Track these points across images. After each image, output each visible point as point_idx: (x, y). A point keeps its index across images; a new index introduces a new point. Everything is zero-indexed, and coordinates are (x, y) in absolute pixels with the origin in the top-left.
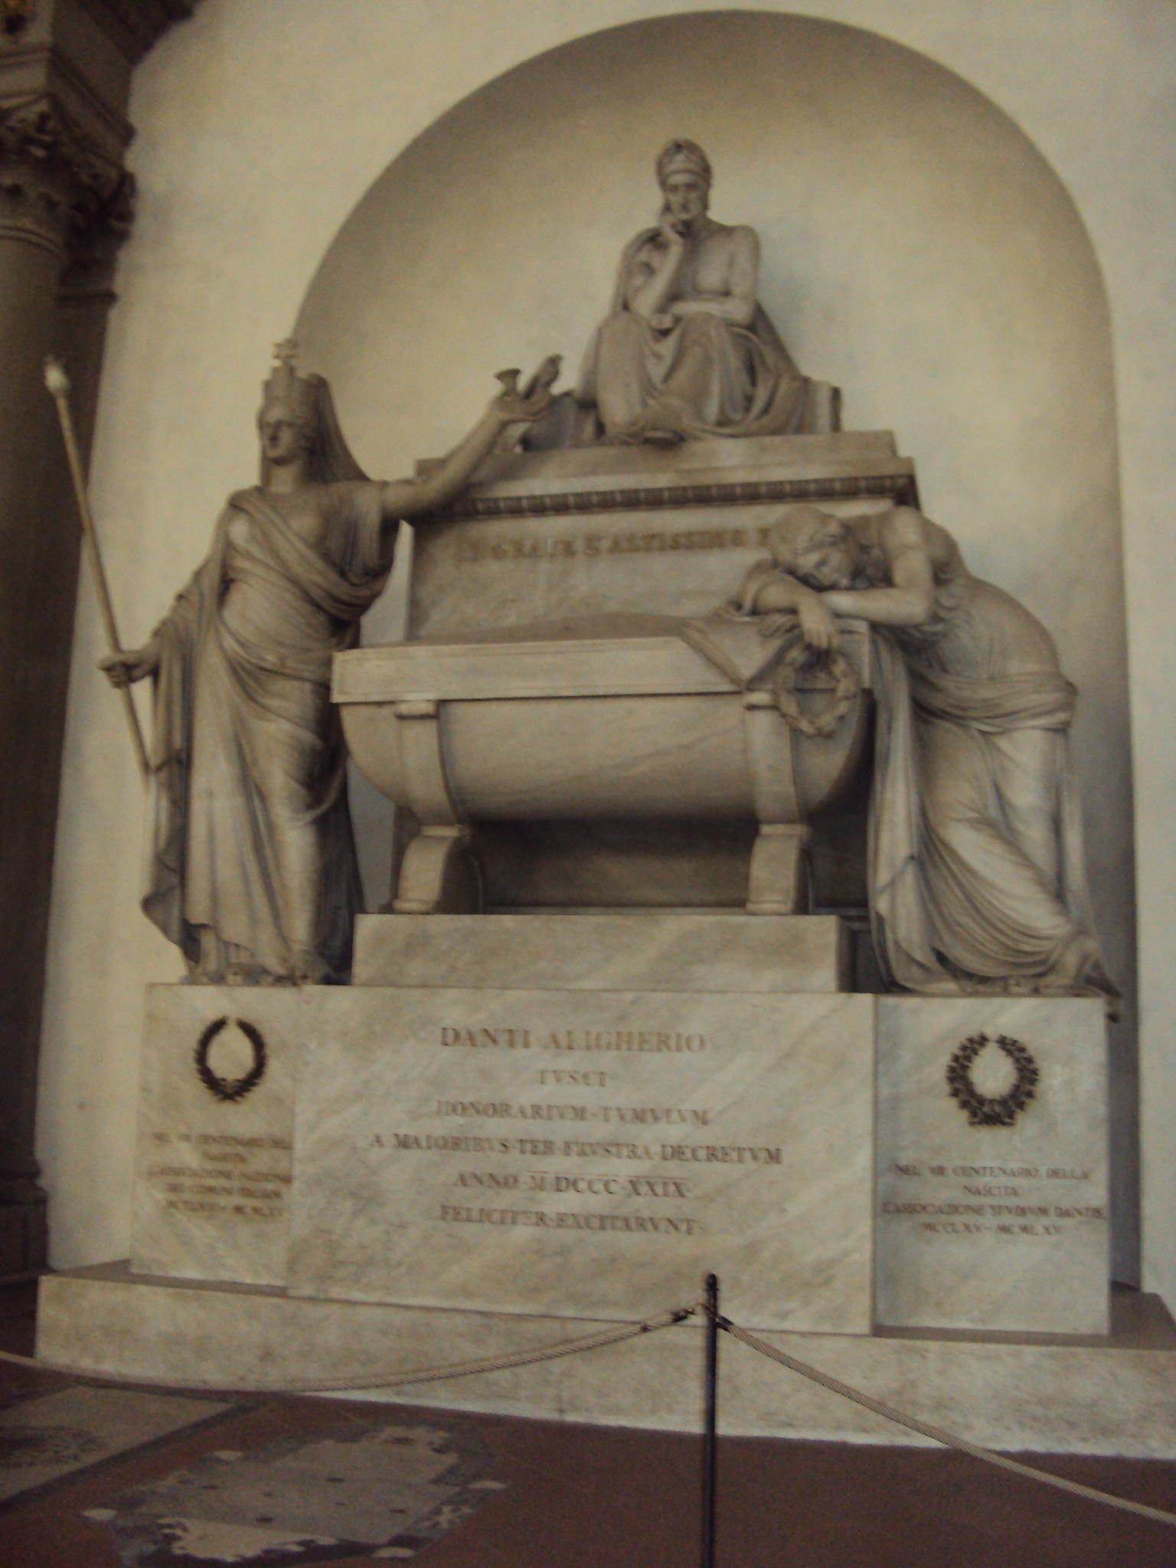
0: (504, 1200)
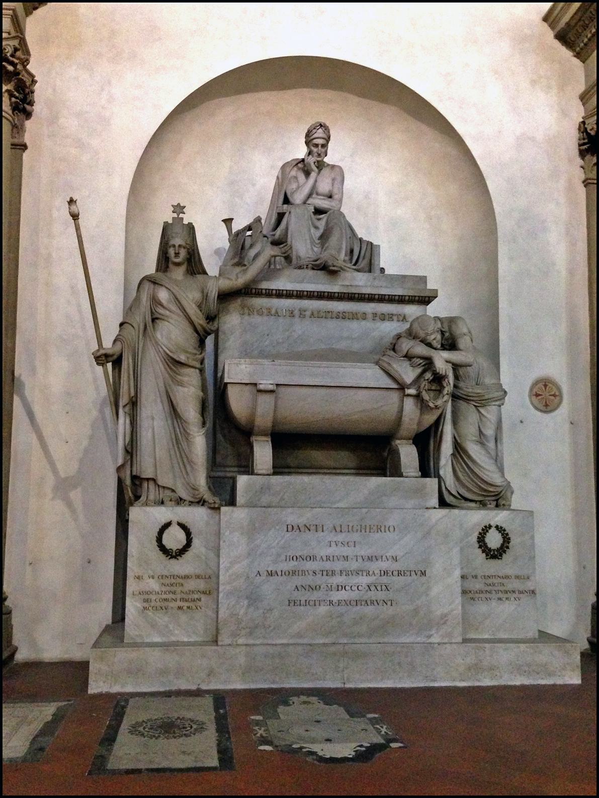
0: (315, 596)
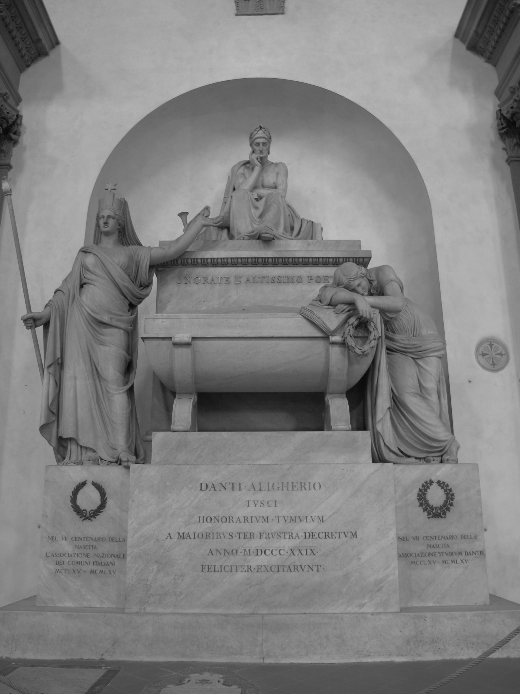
0: (232, 561)
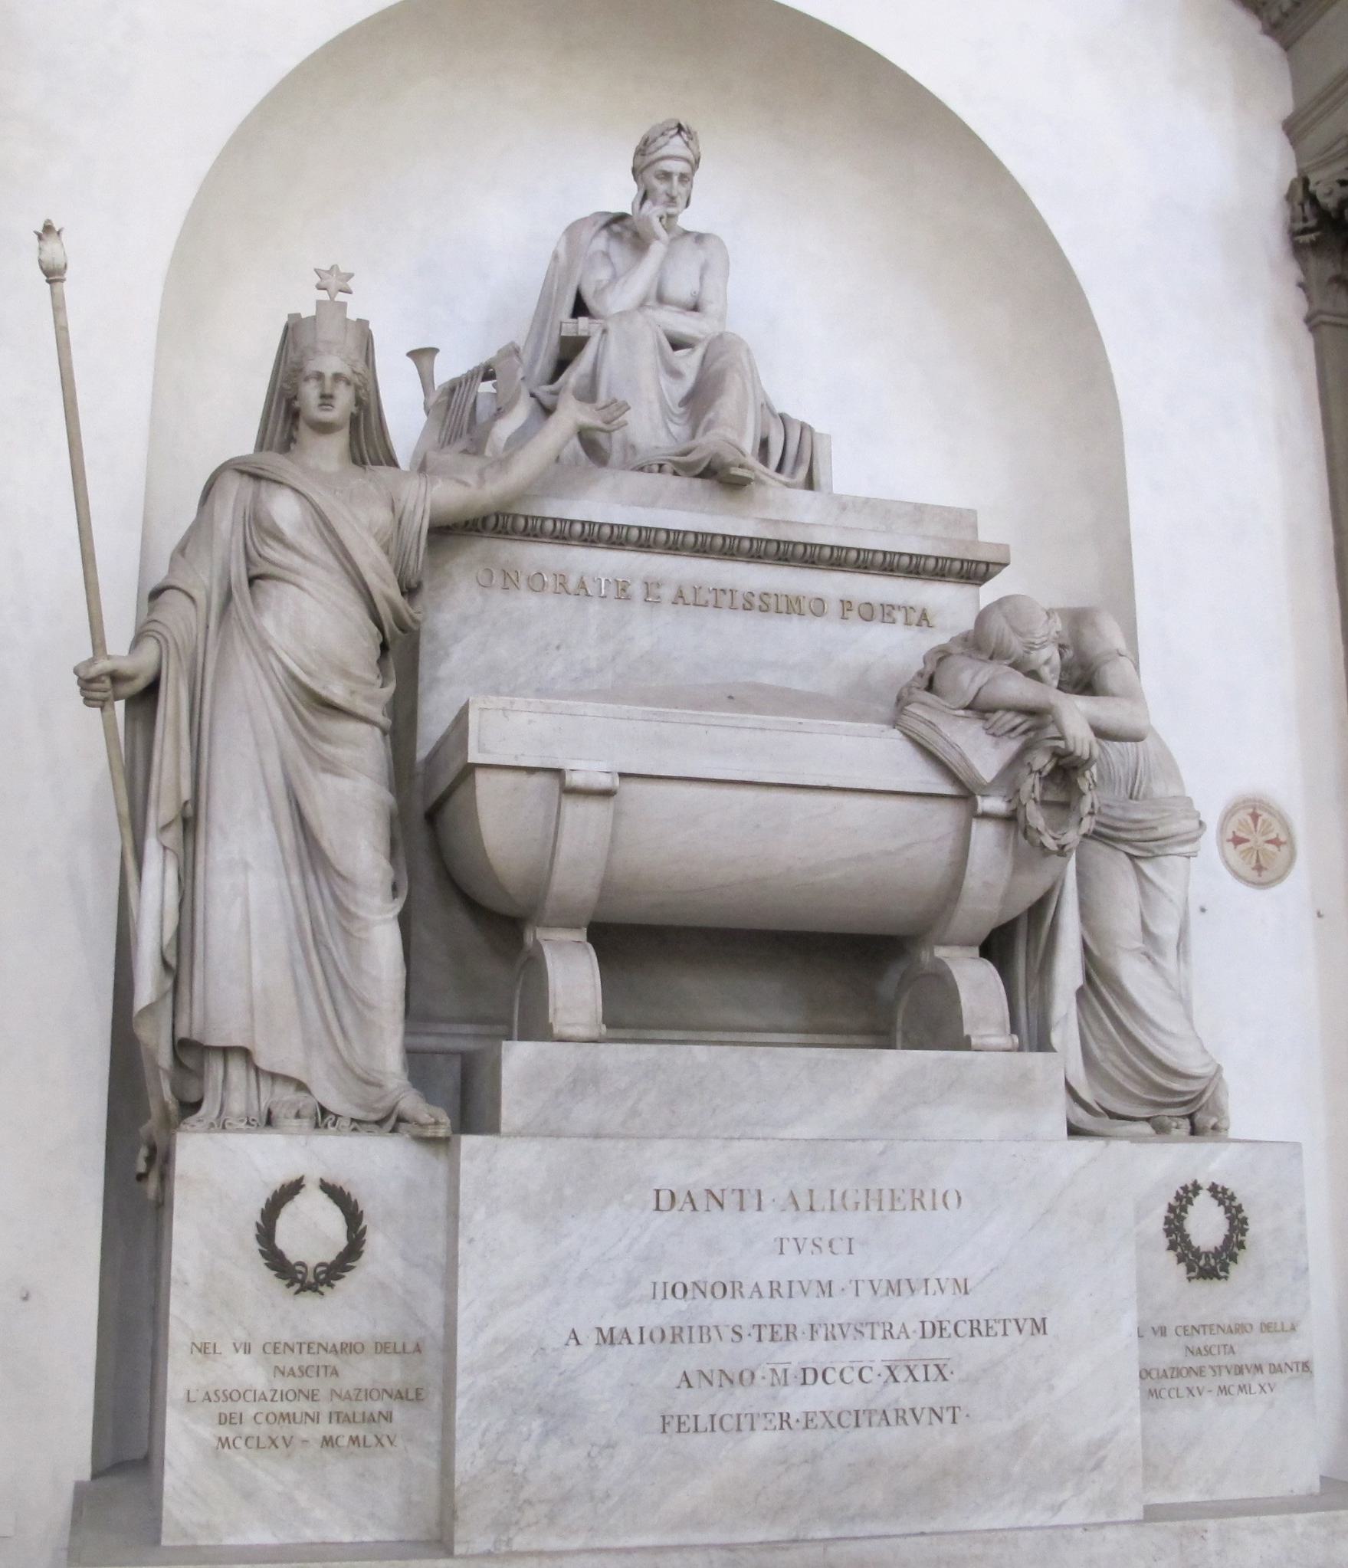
0: (740, 1400)
